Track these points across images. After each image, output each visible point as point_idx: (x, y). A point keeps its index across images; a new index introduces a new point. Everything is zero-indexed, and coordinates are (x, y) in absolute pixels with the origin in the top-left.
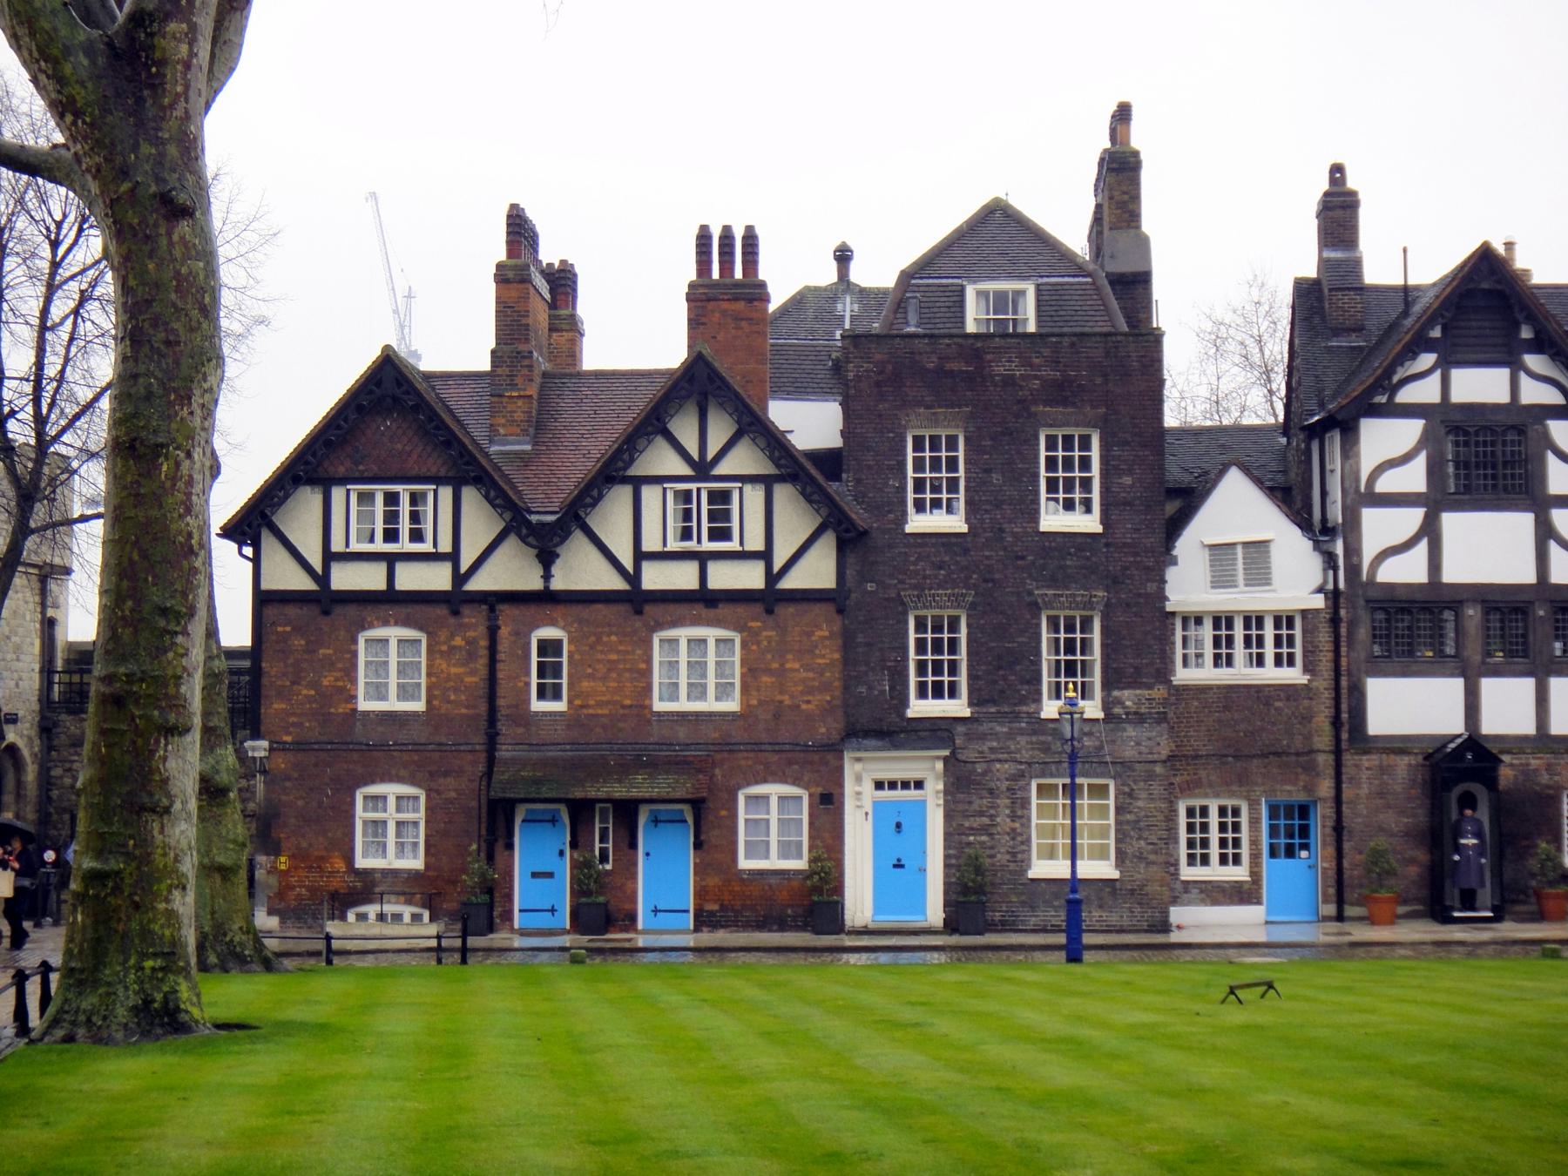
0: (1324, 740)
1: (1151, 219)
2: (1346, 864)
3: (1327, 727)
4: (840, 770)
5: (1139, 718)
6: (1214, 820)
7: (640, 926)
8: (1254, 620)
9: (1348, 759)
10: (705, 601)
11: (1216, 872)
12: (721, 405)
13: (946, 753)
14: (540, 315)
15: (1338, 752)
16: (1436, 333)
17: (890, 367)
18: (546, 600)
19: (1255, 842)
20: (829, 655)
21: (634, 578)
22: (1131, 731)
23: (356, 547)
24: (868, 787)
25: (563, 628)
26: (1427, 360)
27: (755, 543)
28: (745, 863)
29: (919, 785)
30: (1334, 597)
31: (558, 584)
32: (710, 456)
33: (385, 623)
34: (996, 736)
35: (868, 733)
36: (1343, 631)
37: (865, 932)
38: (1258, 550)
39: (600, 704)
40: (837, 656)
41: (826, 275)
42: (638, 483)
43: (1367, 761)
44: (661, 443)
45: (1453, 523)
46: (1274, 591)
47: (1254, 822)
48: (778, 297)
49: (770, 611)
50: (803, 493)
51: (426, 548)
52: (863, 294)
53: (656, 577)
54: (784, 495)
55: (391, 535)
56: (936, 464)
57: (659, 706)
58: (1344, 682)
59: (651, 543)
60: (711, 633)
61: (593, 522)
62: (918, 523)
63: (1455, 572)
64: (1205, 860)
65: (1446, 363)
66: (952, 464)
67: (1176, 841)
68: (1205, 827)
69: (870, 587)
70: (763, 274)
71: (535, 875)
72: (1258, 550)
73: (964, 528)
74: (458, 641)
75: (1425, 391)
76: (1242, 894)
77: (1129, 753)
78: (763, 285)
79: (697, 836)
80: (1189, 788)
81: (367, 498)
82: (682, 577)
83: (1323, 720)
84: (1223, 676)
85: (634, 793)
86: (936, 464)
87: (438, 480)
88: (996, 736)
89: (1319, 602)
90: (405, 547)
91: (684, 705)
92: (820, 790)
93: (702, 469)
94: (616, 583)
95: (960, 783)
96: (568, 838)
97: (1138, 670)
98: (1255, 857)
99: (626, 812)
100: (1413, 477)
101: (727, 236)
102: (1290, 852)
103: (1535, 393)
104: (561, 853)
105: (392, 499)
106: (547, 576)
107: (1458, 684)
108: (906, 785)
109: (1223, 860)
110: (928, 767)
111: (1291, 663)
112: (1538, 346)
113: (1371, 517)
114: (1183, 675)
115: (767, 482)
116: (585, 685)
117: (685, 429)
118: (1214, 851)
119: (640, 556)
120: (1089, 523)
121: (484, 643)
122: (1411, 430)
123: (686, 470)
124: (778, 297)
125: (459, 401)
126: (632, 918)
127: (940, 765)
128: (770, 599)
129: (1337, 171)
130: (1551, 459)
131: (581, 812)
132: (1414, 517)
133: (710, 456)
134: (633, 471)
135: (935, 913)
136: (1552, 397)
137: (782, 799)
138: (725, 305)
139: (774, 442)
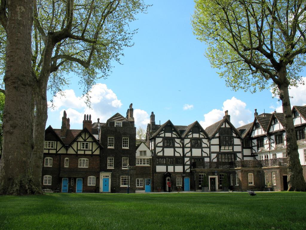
0: (151, 173)
1: (135, 116)
2: (154, 186)
3: (152, 171)
4: (99, 174)
5: (132, 169)
6: (140, 181)
7: (76, 192)
8: (144, 159)
9: (154, 174)
10: (85, 155)
11: (140, 187)
12: (87, 133)
13: (111, 173)
14: (66, 123)
15: (153, 174)
16: (164, 129)
17: (106, 130)
18: (67, 155)
19: (144, 183)
20: (99, 162)
21: (77, 152)
22: (132, 171)
24: (102, 177)
25: (69, 158)
26: (163, 132)
27: (91, 149)
28: (88, 185)
29: (108, 176)
30: (153, 157)
31: (68, 153)
32: (86, 139)
33: (48, 157)
34: (117, 171)
35: (103, 171)
36: (154, 160)
37: (102, 193)
38: (145, 152)
39: (72, 167)
40: (99, 162)
41: (97, 121)
42: (78, 142)
43: (156, 175)
44: (80, 137)
45: (165, 149)
46: (147, 156)
47: (144, 181)
48: (93, 123)
49: (92, 157)
50: (96, 143)
51: (53, 148)
52: (101, 123)
53: (79, 152)
54: (94, 143)
56: (111, 141)
57: (79, 167)
58: (154, 166)
59: (79, 148)
60: (85, 159)
61: (72, 146)
62: (109, 147)
63: (165, 155)
64: (139, 185)
65: (165, 133)
66: (113, 141)
67: (136, 183)
68: (139, 182)
69: (104, 154)
70: (92, 120)
71: (64, 186)
72: (145, 152)
73: (114, 148)
74: (56, 159)
75: (163, 135)
76: (143, 189)
77: (131, 173)
78: (91, 121)
79: (83, 182)
80: (137, 177)
82: (82, 152)
83: (152, 170)
84: (141, 165)
85: (76, 177)
86: (111, 141)
87: (55, 141)
88: (117, 171)
89: (151, 157)
90: (51, 148)
91: (82, 167)
92: (97, 177)
93: (85, 140)
94: (74, 153)
95: (113, 176)
96: (68, 182)
97: (132, 165)
98: (144, 185)
99: (75, 179)
100: (161, 144)
101: (88, 116)
102: (148, 184)
103: (174, 136)
104: (67, 184)
105: (49, 143)
106: (67, 152)
107: (165, 167)
108: (107, 176)
109: (141, 185)
110: (109, 174)
111: (148, 164)
112: (174, 131)
113: (157, 148)
114: (137, 165)
115: (92, 142)
116: (71, 164)
117: (83, 136)
118: (140, 184)
119: (77, 150)
120: (128, 148)
121: (59, 159)
122: (161, 139)
123: (83, 141)
124: (93, 123)
125: (57, 133)
126: (75, 191)
127: (111, 174)
128: (92, 155)
129: (152, 113)
130: (175, 143)
132: (161, 148)
133: (86, 139)
134: (77, 140)
135: (110, 190)
136: (175, 136)
137: (93, 178)
138: (88, 123)
139: (94, 138)
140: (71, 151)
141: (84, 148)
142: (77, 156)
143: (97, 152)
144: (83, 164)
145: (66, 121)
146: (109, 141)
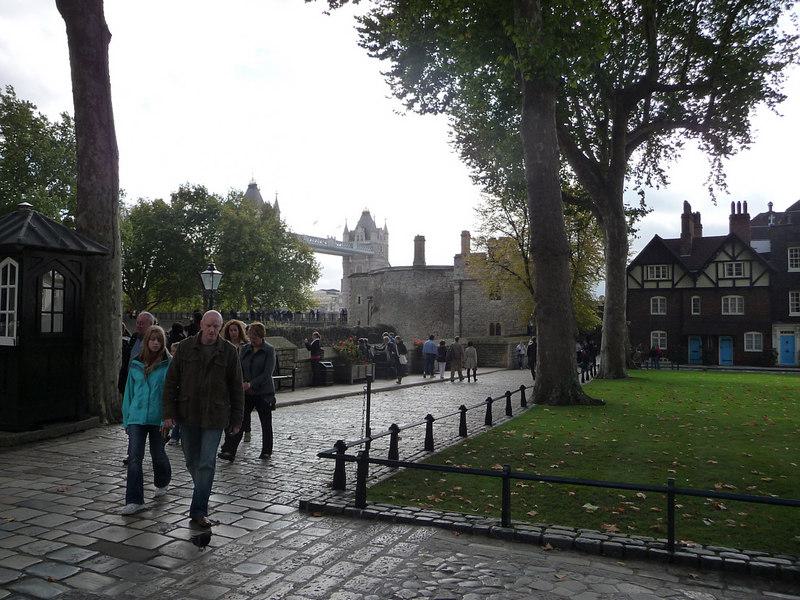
10: (735, 290)
18: (695, 290)
23: (650, 279)
27: (747, 275)
31: (697, 286)
44: (723, 253)
48: (752, 216)
53: (722, 284)
54: (755, 264)
55: (658, 276)
81: (652, 268)
82: (729, 284)
93: (733, 259)
94: (711, 286)
99: (716, 338)
101: (739, 203)
105: (658, 268)
115: (751, 262)
119: (718, 279)
124: (752, 216)
131: (704, 338)
139: (752, 251)
140: (703, 283)
141: (731, 274)
142: (717, 292)
143: (764, 282)
144: (733, 307)
145: (691, 219)
146: (792, 256)
